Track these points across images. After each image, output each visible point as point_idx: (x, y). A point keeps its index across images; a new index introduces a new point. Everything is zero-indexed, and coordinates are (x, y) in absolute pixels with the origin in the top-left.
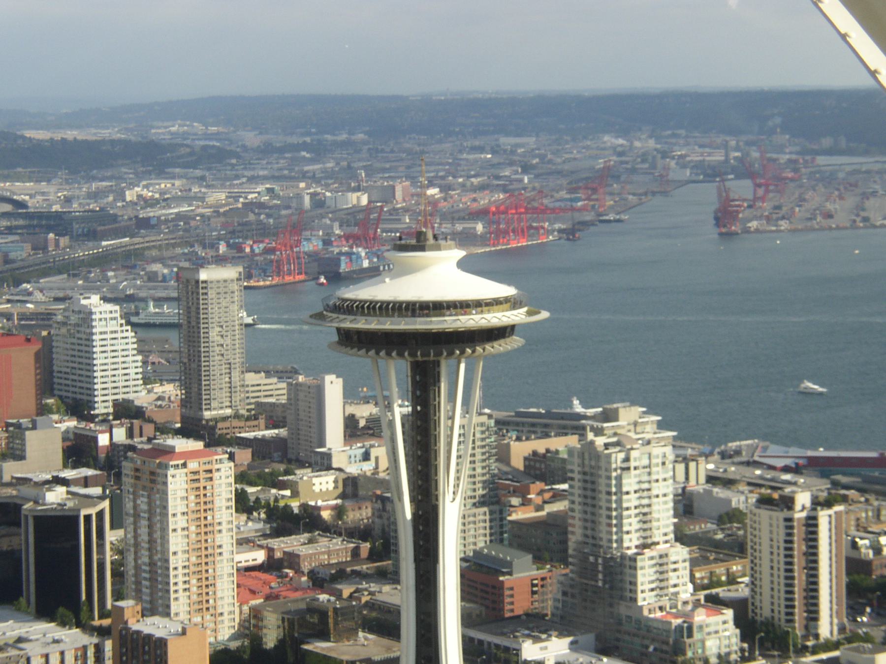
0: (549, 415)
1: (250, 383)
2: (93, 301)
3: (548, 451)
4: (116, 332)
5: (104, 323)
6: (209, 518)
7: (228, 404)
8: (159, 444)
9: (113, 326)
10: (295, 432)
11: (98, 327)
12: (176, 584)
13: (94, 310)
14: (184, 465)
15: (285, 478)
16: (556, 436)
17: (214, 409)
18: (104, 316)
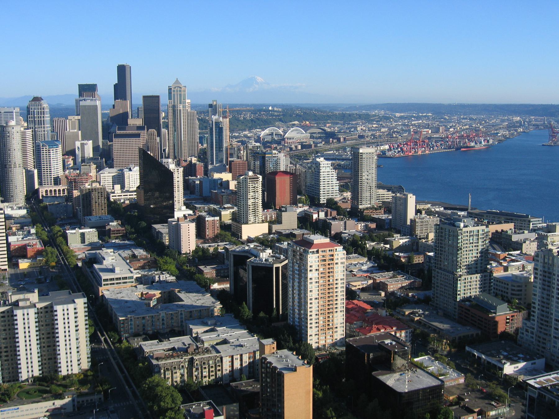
0: (501, 214)
1: (381, 194)
2: (321, 160)
3: (502, 231)
4: (329, 172)
5: (324, 168)
6: (331, 280)
7: (369, 203)
8: (306, 238)
9: (328, 169)
10: (395, 217)
11: (322, 170)
12: (311, 315)
13: (321, 163)
14: (317, 252)
15: (388, 239)
16: (504, 223)
18: (324, 166)
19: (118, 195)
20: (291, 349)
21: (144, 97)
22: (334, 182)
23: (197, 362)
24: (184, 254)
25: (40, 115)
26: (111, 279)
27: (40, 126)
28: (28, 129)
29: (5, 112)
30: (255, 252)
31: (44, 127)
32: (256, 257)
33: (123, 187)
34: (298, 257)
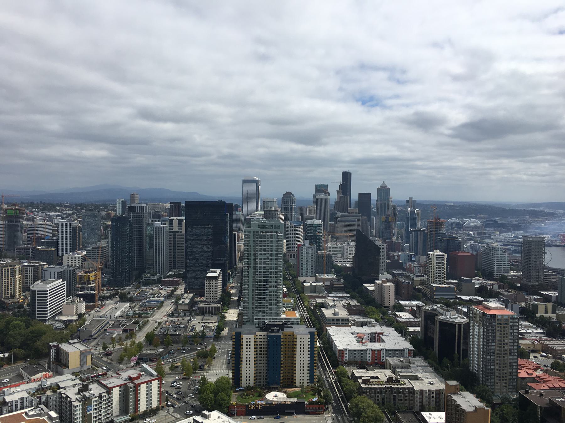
4: (502, 254)
5: (498, 251)
17: (532, 282)
19: (339, 261)
20: (472, 393)
21: (359, 194)
22: (506, 263)
23: (395, 390)
24: (385, 307)
25: (290, 204)
26: (333, 320)
27: (289, 211)
28: (282, 213)
29: (267, 201)
30: (442, 311)
31: (292, 212)
32: (442, 315)
33: (343, 256)
34: (478, 319)
